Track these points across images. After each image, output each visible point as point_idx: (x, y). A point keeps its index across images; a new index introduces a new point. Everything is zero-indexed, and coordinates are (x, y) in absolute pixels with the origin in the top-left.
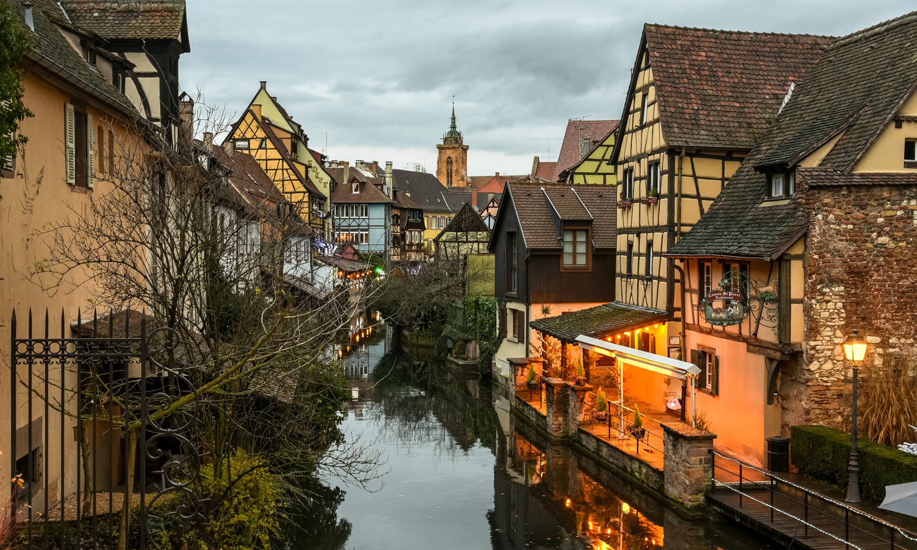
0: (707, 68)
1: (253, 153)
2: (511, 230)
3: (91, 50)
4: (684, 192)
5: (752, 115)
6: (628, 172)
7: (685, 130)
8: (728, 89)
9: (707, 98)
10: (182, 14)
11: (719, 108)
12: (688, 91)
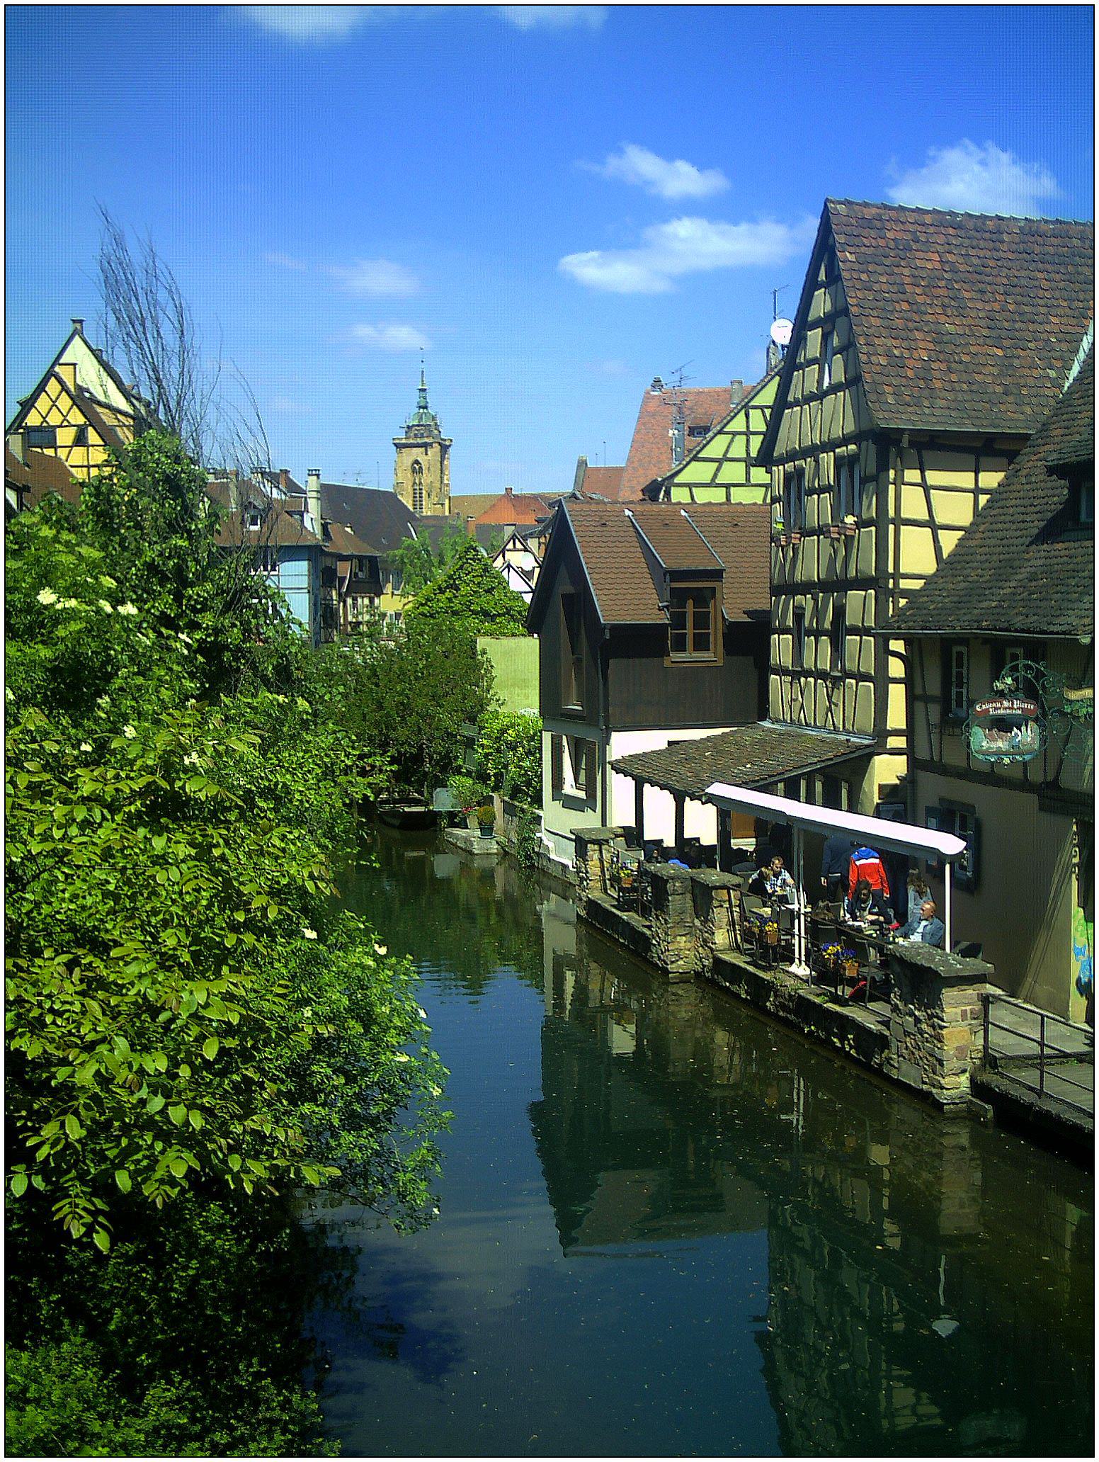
0: (942, 284)
1: (62, 453)
2: (569, 589)
5: (1027, 372)
6: (793, 479)
8: (983, 323)
11: (965, 358)
12: (911, 325)
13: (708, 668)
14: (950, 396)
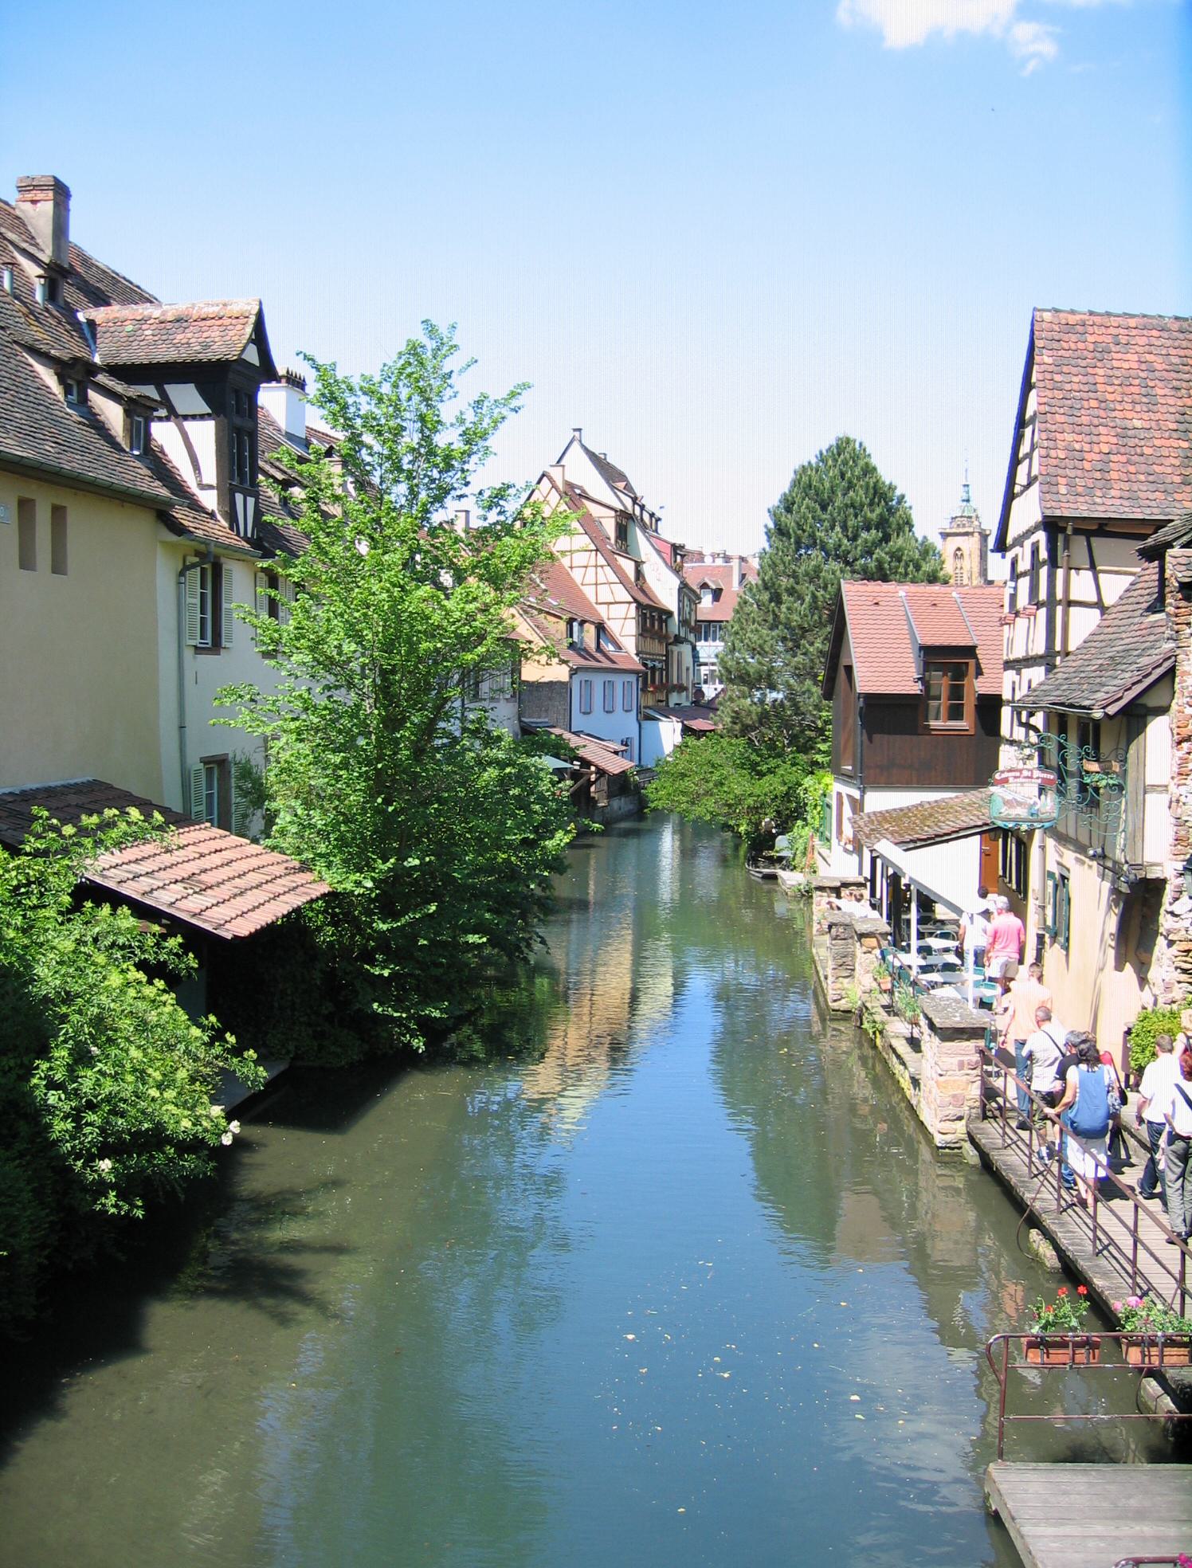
0: (1137, 382)
3: (79, 383)
4: (1072, 597)
7: (1080, 489)
9: (1130, 433)
10: (253, 319)
13: (959, 735)
14: (1126, 486)
